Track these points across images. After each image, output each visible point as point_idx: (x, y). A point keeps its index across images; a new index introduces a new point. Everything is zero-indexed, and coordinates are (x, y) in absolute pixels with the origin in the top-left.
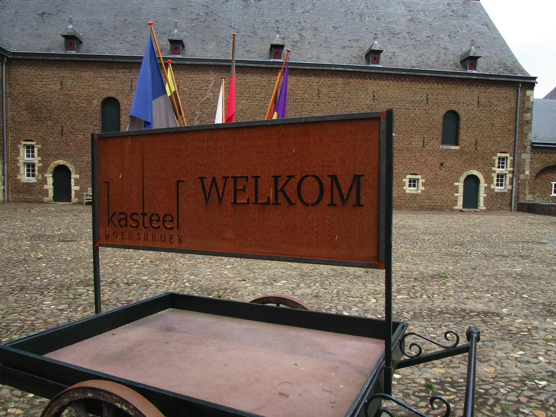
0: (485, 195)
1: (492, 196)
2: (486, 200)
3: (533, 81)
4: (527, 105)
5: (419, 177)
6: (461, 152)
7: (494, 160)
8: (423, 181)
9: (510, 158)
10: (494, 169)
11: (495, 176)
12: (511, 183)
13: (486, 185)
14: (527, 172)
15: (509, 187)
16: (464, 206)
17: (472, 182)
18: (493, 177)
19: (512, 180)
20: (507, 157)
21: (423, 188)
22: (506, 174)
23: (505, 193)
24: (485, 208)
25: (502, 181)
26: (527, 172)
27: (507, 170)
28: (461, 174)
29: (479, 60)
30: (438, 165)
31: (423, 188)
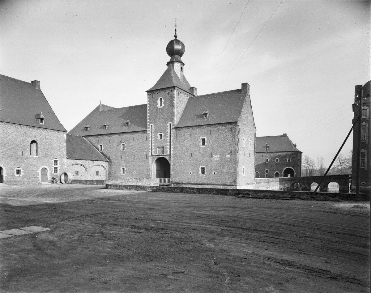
7: (53, 162)
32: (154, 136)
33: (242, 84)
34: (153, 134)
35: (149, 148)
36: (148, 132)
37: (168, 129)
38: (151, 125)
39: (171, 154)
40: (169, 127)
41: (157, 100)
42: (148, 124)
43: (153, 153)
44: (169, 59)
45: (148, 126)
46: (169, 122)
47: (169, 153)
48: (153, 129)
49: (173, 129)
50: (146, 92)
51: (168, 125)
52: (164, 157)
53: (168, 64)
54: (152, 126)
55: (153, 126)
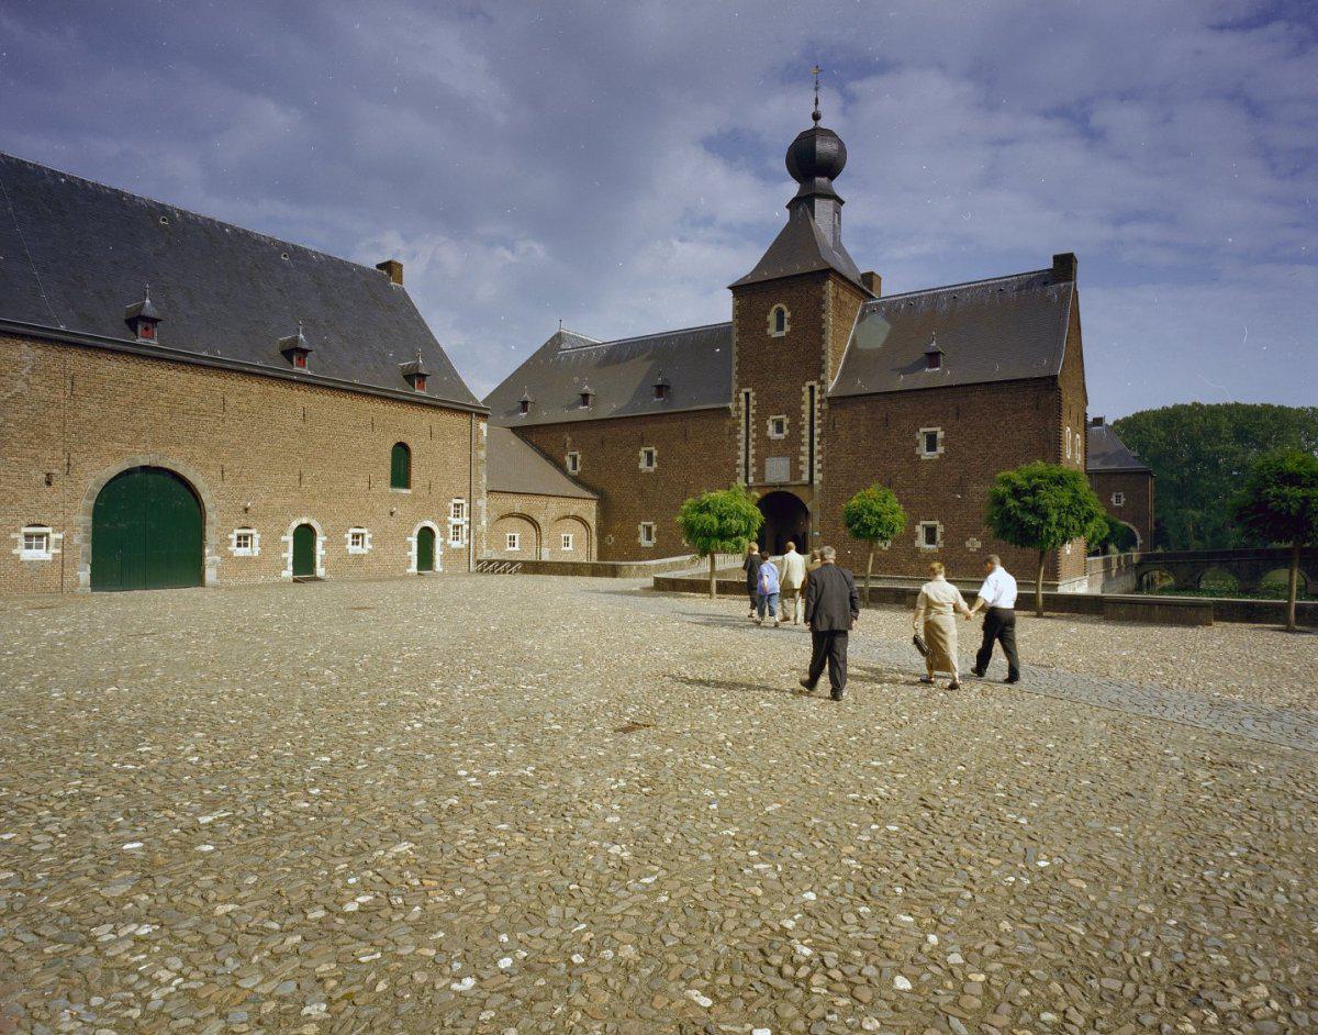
1: (450, 554)
2: (444, 558)
5: (365, 531)
6: (414, 498)
8: (371, 536)
9: (466, 506)
10: (450, 518)
11: (450, 527)
13: (442, 539)
14: (484, 523)
16: (419, 568)
17: (426, 537)
21: (371, 547)
25: (457, 533)
26: (484, 523)
27: (463, 520)
28: (413, 526)
30: (388, 514)
31: (371, 547)
32: (755, 427)
33: (1056, 258)
34: (752, 420)
35: (738, 462)
36: (734, 413)
39: (816, 482)
41: (767, 313)
42: (735, 386)
43: (751, 479)
44: (793, 188)
45: (734, 396)
46: (807, 380)
47: (806, 477)
48: (753, 402)
49: (821, 401)
50: (730, 288)
51: (806, 390)
52: (790, 491)
53: (793, 205)
54: (747, 394)
55: (752, 395)
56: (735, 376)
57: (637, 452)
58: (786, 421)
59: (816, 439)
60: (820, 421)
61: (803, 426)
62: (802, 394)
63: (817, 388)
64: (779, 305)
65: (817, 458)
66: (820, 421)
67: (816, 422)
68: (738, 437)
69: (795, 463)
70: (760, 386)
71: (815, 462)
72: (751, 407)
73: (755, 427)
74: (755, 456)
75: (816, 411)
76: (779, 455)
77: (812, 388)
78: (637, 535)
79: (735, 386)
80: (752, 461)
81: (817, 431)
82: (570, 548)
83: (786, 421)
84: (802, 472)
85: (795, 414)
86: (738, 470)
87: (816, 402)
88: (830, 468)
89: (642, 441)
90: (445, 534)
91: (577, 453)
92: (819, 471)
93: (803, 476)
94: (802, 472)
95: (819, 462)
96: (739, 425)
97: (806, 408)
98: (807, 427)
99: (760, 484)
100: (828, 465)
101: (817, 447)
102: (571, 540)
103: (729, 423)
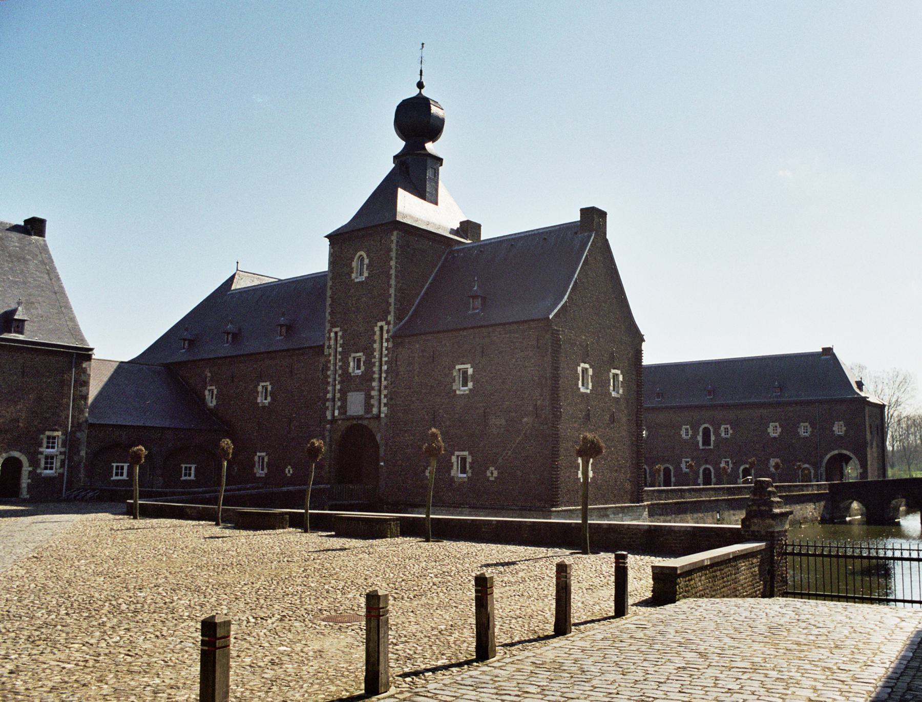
0: (30, 481)
3: (90, 353)
4: (83, 378)
7: (42, 439)
10: (41, 450)
12: (62, 465)
13: (31, 469)
14: (83, 453)
15: (61, 471)
18: (40, 459)
19: (63, 462)
20: (58, 436)
22: (57, 456)
23: (55, 478)
24: (28, 496)
25: (52, 463)
26: (83, 453)
29: (26, 323)
33: (582, 210)
34: (339, 357)
36: (326, 352)
37: (375, 342)
38: (335, 330)
39: (382, 415)
40: (377, 337)
41: (352, 259)
42: (328, 326)
49: (387, 340)
50: (326, 237)
51: (377, 329)
52: (366, 422)
54: (336, 333)
55: (340, 334)
56: (328, 317)
57: (256, 386)
58: (363, 359)
59: (384, 375)
60: (386, 359)
61: (375, 362)
62: (374, 333)
63: (385, 328)
64: (358, 254)
65: (385, 392)
66: (386, 359)
67: (385, 359)
68: (329, 373)
69: (368, 397)
70: (346, 327)
71: (383, 396)
72: (338, 345)
73: (340, 364)
74: (340, 391)
75: (384, 349)
76: (358, 390)
77: (381, 328)
78: (254, 465)
79: (328, 326)
80: (338, 395)
81: (385, 367)
82: (192, 477)
83: (363, 359)
84: (373, 406)
85: (370, 354)
86: (327, 404)
87: (384, 341)
88: (393, 402)
89: (261, 378)
90: (34, 463)
91: (213, 387)
92: (385, 405)
93: (374, 409)
94: (373, 406)
95: (386, 396)
96: (330, 361)
97: (376, 346)
98: (377, 364)
99: (342, 417)
100: (390, 397)
101: (384, 383)
102: (193, 469)
103: (323, 360)
